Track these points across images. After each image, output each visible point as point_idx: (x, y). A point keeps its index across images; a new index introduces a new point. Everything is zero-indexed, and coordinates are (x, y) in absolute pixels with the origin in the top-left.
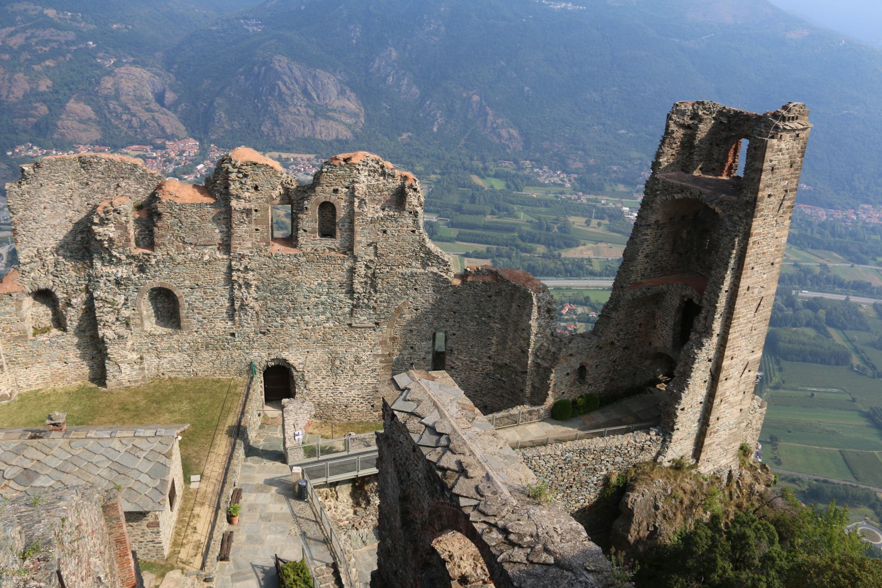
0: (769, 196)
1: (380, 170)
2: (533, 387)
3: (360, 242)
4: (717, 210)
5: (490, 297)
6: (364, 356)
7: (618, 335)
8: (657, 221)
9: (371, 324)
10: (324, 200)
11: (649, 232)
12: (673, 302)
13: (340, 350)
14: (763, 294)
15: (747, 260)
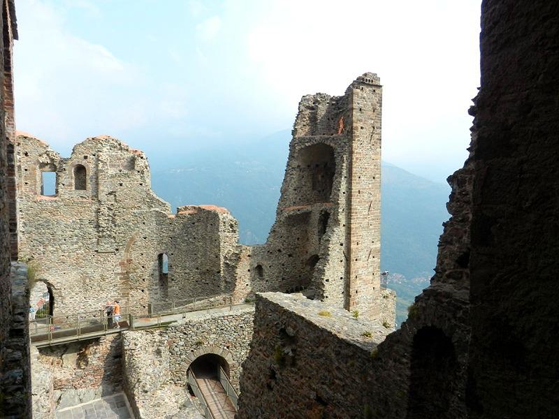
0: (362, 128)
1: (119, 147)
2: (226, 282)
3: (103, 191)
4: (331, 144)
5: (194, 224)
6: (107, 274)
7: (283, 245)
8: (299, 166)
9: (112, 250)
10: (77, 163)
11: (294, 172)
12: (316, 217)
13: (89, 271)
14: (372, 199)
15: (354, 170)
